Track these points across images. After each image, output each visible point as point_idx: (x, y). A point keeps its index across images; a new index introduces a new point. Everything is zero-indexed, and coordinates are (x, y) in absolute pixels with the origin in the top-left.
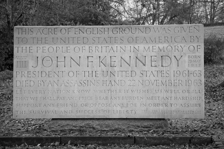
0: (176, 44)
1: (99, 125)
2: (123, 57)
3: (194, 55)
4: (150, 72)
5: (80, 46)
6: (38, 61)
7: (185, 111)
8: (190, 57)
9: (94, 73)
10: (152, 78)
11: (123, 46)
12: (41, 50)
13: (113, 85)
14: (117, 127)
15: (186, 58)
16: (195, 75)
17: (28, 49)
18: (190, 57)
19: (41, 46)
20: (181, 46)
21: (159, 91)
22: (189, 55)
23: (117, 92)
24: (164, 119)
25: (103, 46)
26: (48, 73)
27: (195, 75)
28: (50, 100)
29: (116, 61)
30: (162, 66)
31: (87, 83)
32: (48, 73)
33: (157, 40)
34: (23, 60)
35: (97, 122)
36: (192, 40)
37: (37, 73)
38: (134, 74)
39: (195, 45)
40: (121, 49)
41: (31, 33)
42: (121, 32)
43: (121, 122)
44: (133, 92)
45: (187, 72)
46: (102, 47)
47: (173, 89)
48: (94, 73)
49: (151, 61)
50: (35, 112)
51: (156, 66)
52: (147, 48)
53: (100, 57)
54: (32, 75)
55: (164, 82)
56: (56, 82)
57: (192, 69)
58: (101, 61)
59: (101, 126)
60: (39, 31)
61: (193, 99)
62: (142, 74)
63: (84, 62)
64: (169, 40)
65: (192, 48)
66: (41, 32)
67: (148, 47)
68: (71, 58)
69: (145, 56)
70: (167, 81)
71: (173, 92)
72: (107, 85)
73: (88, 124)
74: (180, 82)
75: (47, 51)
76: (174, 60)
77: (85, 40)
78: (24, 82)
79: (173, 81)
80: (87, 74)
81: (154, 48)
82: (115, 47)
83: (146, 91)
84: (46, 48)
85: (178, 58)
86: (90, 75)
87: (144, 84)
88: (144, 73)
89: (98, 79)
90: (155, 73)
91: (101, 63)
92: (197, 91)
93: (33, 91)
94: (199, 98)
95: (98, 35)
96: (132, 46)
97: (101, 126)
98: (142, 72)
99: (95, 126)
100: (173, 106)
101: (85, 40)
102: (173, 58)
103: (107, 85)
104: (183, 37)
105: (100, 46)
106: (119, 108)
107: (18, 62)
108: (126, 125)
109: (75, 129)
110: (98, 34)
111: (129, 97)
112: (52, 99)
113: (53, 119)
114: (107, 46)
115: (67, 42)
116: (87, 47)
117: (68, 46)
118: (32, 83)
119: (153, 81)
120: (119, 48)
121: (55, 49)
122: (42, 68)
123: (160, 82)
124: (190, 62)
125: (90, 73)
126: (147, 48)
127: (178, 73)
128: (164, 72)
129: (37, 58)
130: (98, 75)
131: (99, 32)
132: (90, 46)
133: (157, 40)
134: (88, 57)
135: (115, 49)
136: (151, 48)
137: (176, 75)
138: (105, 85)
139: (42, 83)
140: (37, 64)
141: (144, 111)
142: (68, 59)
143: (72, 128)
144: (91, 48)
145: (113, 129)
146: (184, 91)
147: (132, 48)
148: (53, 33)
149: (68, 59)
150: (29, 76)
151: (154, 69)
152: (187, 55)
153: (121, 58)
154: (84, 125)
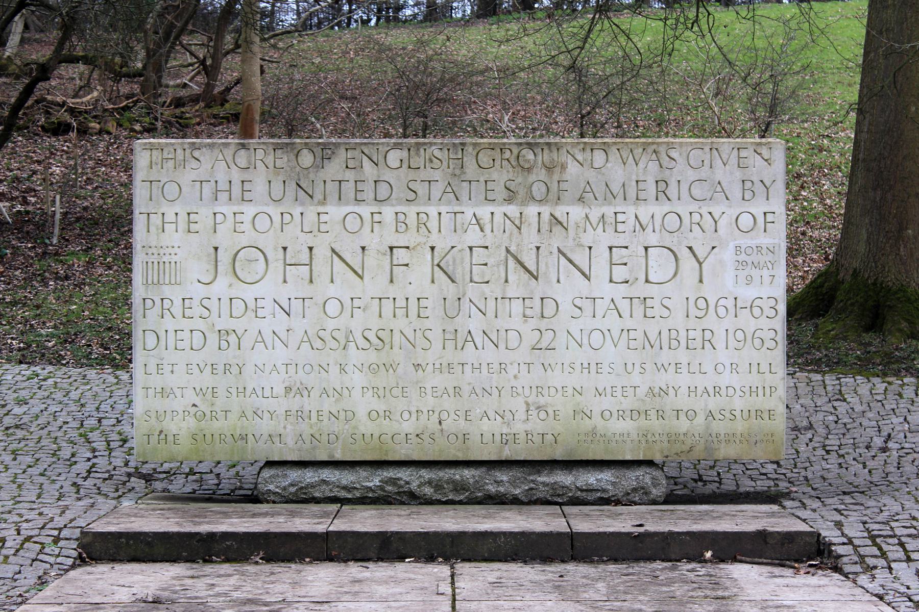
0: (694, 207)
1: (430, 483)
2: (513, 249)
3: (753, 243)
4: (607, 300)
5: (365, 211)
6: (216, 261)
7: (723, 435)
8: (743, 250)
9: (413, 303)
10: (613, 322)
13: (480, 346)
14: (492, 489)
15: (727, 255)
16: (756, 311)
17: (183, 217)
18: (743, 250)
19: (228, 210)
20: (710, 213)
21: (637, 366)
22: (737, 243)
23: (491, 371)
24: (650, 463)
25: (443, 209)
26: (251, 305)
27: (756, 311)
28: (260, 396)
29: (491, 262)
30: (647, 281)
31: (387, 340)
32: (251, 305)
33: (632, 193)
34: (165, 259)
35: (426, 474)
36: (748, 195)
37: (213, 305)
38: (550, 309)
39: (758, 211)
40: (507, 221)
41: (195, 164)
42: (505, 163)
43: (503, 476)
44: (549, 370)
45: (730, 303)
46: (440, 214)
47: (685, 361)
48: (413, 303)
49: (611, 264)
50: (208, 437)
51: (627, 282)
52: (594, 218)
53: (433, 248)
54: (198, 310)
55: (653, 336)
56: (283, 335)
57: (748, 293)
58: (436, 262)
60: (221, 157)
61: (748, 394)
62: (580, 308)
63: (376, 263)
64: (672, 191)
65: (746, 221)
66: (229, 159)
67: (600, 215)
68: (333, 250)
69: (590, 248)
70: (665, 334)
71: (684, 370)
72: (460, 346)
73: (393, 481)
74: (708, 334)
75: (248, 226)
76: (688, 264)
78: (171, 334)
79: (683, 333)
80: (388, 306)
81: (620, 218)
82: (484, 211)
83: (593, 367)
84: (247, 219)
85: (701, 253)
87: (585, 341)
89: (427, 324)
90: (624, 306)
91: (436, 268)
92: (764, 368)
93: (202, 366)
94: (768, 391)
97: (438, 486)
98: (578, 302)
99: (419, 486)
100: (682, 416)
101: (383, 191)
102: (684, 253)
103: (460, 346)
104: (719, 183)
105: (433, 211)
107: (150, 264)
108: (523, 483)
109: (350, 496)
110: (428, 169)
111: (534, 389)
112: (267, 393)
113: (270, 464)
114: (457, 209)
115: (318, 196)
116: (388, 212)
117: (321, 209)
118: (198, 337)
119: (616, 333)
120: (498, 218)
121: (277, 219)
122: (230, 285)
123: (639, 335)
124: (741, 267)
125: (401, 303)
126: (594, 218)
128: (656, 303)
129: (213, 250)
130: (428, 313)
131: (431, 161)
132: (399, 209)
133: (632, 193)
134: (391, 248)
136: (610, 219)
137: (693, 312)
138: (450, 345)
139: (232, 338)
140: (213, 271)
141: (586, 434)
142: (323, 253)
143: (339, 494)
144: (401, 217)
145: (477, 497)
146: (720, 368)
147: (546, 217)
148: (271, 166)
149: (323, 253)
150: (188, 312)
152: (732, 246)
153: (508, 251)
154: (378, 484)
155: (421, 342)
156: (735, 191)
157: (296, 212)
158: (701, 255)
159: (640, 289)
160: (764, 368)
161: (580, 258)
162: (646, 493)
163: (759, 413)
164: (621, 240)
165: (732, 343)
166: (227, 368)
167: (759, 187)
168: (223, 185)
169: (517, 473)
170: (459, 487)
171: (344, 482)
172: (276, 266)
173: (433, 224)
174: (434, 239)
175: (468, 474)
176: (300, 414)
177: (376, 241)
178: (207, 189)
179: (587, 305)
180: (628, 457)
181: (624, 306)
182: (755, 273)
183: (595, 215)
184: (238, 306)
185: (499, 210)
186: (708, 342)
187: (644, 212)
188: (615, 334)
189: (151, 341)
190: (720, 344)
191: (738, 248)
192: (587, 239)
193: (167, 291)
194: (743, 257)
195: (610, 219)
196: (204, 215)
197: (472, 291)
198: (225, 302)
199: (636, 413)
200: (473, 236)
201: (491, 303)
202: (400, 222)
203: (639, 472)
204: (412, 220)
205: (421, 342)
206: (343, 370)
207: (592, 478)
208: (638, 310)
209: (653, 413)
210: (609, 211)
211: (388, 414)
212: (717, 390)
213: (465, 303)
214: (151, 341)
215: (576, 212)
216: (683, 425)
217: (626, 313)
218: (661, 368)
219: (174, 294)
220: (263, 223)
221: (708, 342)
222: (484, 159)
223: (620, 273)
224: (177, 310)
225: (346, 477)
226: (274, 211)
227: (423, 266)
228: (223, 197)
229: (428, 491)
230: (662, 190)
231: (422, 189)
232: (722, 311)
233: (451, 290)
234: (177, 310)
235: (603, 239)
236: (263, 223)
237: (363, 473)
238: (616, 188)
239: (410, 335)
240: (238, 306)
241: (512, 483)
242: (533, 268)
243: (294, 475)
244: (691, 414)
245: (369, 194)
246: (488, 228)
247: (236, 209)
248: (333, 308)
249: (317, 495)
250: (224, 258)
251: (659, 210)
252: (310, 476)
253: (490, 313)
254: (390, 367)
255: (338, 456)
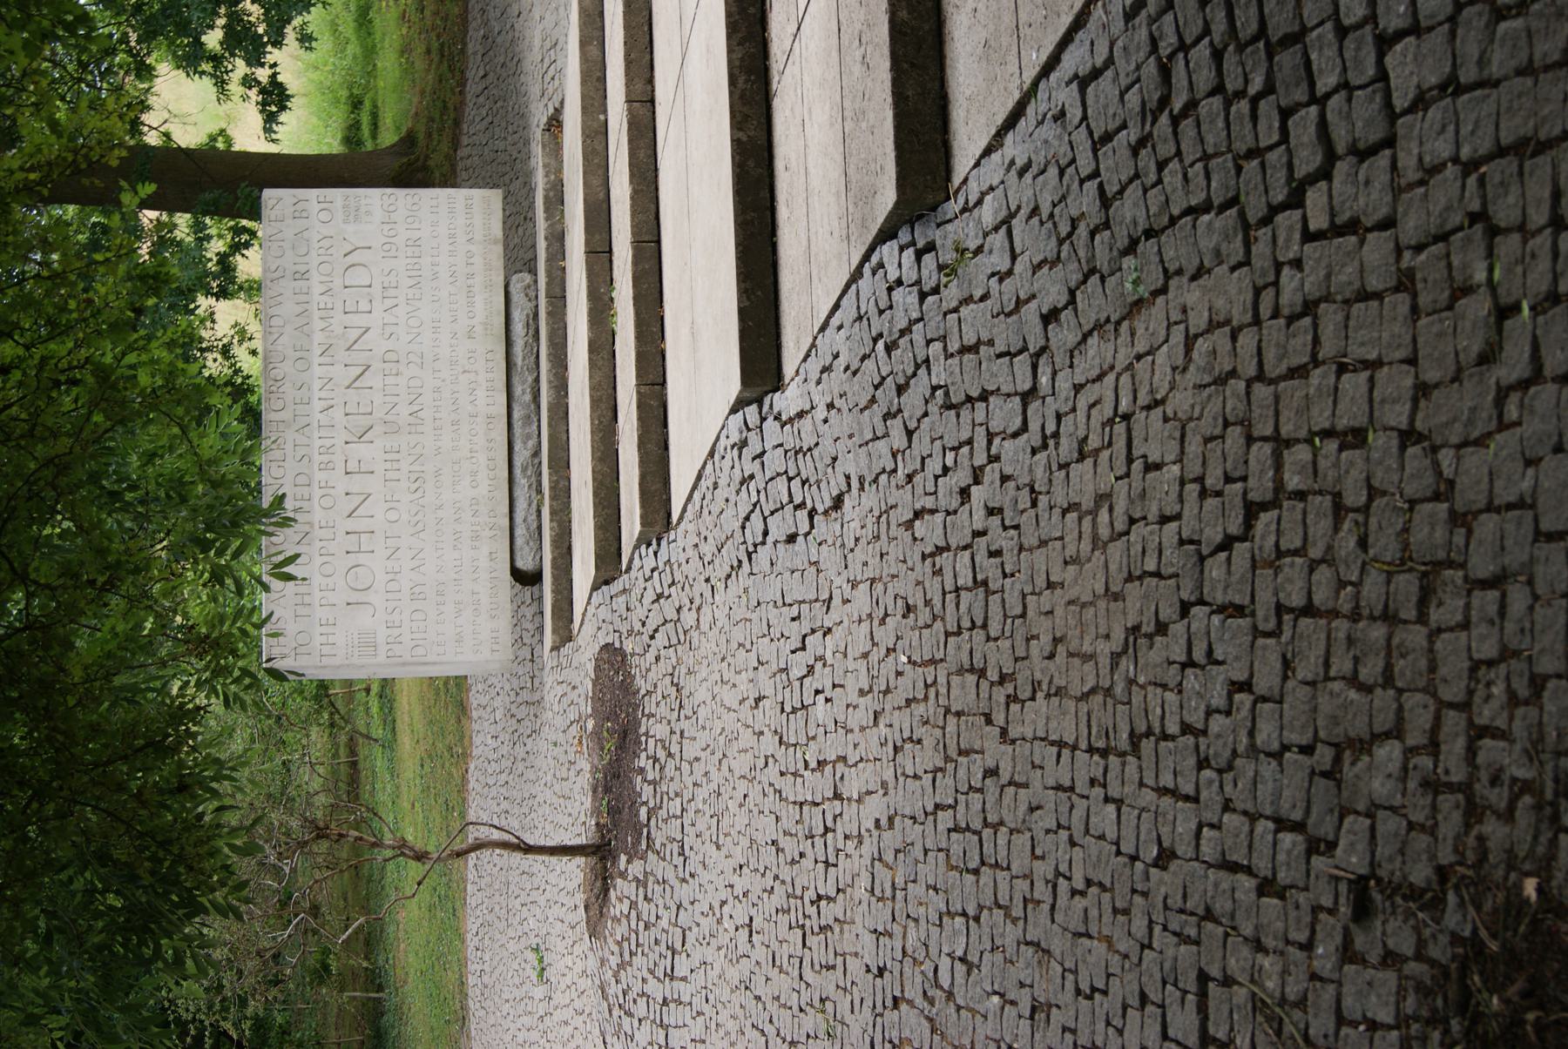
0: (313, 253)
5: (317, 493)
9: (388, 456)
11: (317, 385)
12: (329, 594)
14: (528, 397)
15: (350, 228)
17: (324, 630)
19: (317, 595)
24: (507, 286)
25: (316, 435)
26: (391, 576)
32: (391, 576)
33: (303, 298)
35: (518, 446)
37: (391, 605)
45: (387, 227)
48: (388, 456)
52: (323, 324)
55: (412, 282)
56: (414, 552)
59: (528, 437)
63: (357, 484)
64: (302, 269)
65: (324, 216)
73: (524, 469)
77: (302, 480)
80: (390, 475)
82: (318, 405)
86: (396, 466)
88: (388, 330)
90: (389, 303)
92: (434, 202)
95: (289, 447)
96: (317, 360)
97: (528, 437)
101: (302, 480)
102: (350, 259)
106: (481, 394)
115: (307, 528)
116: (319, 476)
118: (416, 616)
120: (323, 394)
121: (325, 559)
125: (388, 465)
126: (323, 324)
127: (386, 247)
132: (316, 467)
133: (303, 298)
135: (324, 404)
136: (323, 314)
137: (393, 253)
138: (420, 429)
139: (417, 590)
142: (351, 525)
147: (322, 360)
149: (351, 525)
151: (378, 307)
155: (418, 450)
156: (302, 223)
157: (319, 544)
158: (350, 248)
159: (377, 289)
160: (434, 202)
161: (354, 334)
162: (529, 286)
163: (469, 207)
164: (339, 306)
165: (416, 226)
166: (440, 594)
167: (300, 206)
168: (299, 599)
169: (516, 380)
170: (527, 419)
171: (525, 505)
172: (362, 558)
173: (328, 443)
174: (339, 442)
175: (516, 415)
176: (476, 537)
177: (341, 484)
178: (301, 611)
179: (388, 330)
180: (502, 299)
181: (389, 303)
182: (363, 209)
183: (320, 324)
184: (393, 586)
185: (317, 395)
186: (416, 243)
187: (317, 289)
188: (410, 309)
189: (420, 651)
190: (417, 234)
191: (345, 222)
192: (339, 330)
193: (381, 639)
194: (351, 218)
195: (323, 314)
196: (322, 613)
197: (379, 414)
198: (390, 596)
199: (470, 294)
200: (337, 414)
201: (388, 399)
202: (326, 467)
203: (512, 289)
204: (325, 458)
205: (418, 450)
206: (440, 507)
207: (519, 328)
208: (392, 292)
209: (470, 282)
210: (317, 314)
211: (474, 474)
212: (452, 236)
213: (388, 418)
214: (420, 651)
215: (318, 337)
216: (478, 260)
217: (395, 301)
218: (435, 277)
219: (382, 635)
220: (328, 569)
221: (416, 243)
222: (280, 404)
223: (364, 306)
224: (396, 632)
225: (521, 505)
226: (318, 560)
227: (361, 450)
228: (307, 599)
229: (531, 443)
230: (303, 276)
231: (301, 451)
232: (392, 233)
233: (378, 429)
234: (396, 632)
235: (338, 319)
236: (328, 569)
237: (518, 493)
238: (299, 309)
239: (412, 459)
240: (393, 586)
241: (523, 383)
242: (360, 370)
243: (519, 542)
244: (469, 253)
245: (305, 491)
246: (331, 402)
247: (317, 591)
248: (393, 516)
249: (535, 525)
250: (355, 596)
251: (315, 277)
252: (520, 531)
253: (395, 399)
254: (438, 473)
255: (506, 510)
